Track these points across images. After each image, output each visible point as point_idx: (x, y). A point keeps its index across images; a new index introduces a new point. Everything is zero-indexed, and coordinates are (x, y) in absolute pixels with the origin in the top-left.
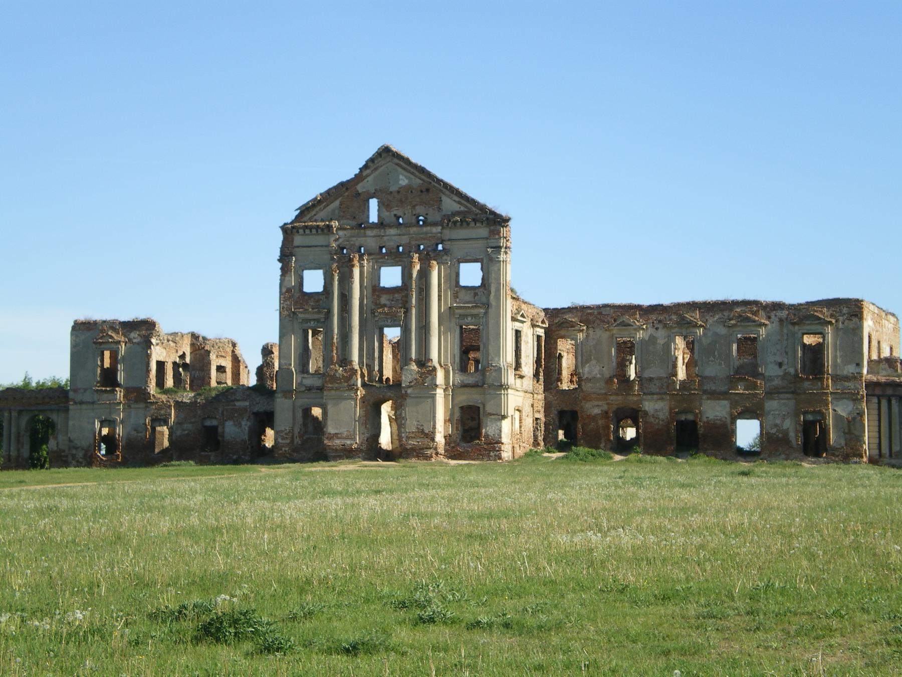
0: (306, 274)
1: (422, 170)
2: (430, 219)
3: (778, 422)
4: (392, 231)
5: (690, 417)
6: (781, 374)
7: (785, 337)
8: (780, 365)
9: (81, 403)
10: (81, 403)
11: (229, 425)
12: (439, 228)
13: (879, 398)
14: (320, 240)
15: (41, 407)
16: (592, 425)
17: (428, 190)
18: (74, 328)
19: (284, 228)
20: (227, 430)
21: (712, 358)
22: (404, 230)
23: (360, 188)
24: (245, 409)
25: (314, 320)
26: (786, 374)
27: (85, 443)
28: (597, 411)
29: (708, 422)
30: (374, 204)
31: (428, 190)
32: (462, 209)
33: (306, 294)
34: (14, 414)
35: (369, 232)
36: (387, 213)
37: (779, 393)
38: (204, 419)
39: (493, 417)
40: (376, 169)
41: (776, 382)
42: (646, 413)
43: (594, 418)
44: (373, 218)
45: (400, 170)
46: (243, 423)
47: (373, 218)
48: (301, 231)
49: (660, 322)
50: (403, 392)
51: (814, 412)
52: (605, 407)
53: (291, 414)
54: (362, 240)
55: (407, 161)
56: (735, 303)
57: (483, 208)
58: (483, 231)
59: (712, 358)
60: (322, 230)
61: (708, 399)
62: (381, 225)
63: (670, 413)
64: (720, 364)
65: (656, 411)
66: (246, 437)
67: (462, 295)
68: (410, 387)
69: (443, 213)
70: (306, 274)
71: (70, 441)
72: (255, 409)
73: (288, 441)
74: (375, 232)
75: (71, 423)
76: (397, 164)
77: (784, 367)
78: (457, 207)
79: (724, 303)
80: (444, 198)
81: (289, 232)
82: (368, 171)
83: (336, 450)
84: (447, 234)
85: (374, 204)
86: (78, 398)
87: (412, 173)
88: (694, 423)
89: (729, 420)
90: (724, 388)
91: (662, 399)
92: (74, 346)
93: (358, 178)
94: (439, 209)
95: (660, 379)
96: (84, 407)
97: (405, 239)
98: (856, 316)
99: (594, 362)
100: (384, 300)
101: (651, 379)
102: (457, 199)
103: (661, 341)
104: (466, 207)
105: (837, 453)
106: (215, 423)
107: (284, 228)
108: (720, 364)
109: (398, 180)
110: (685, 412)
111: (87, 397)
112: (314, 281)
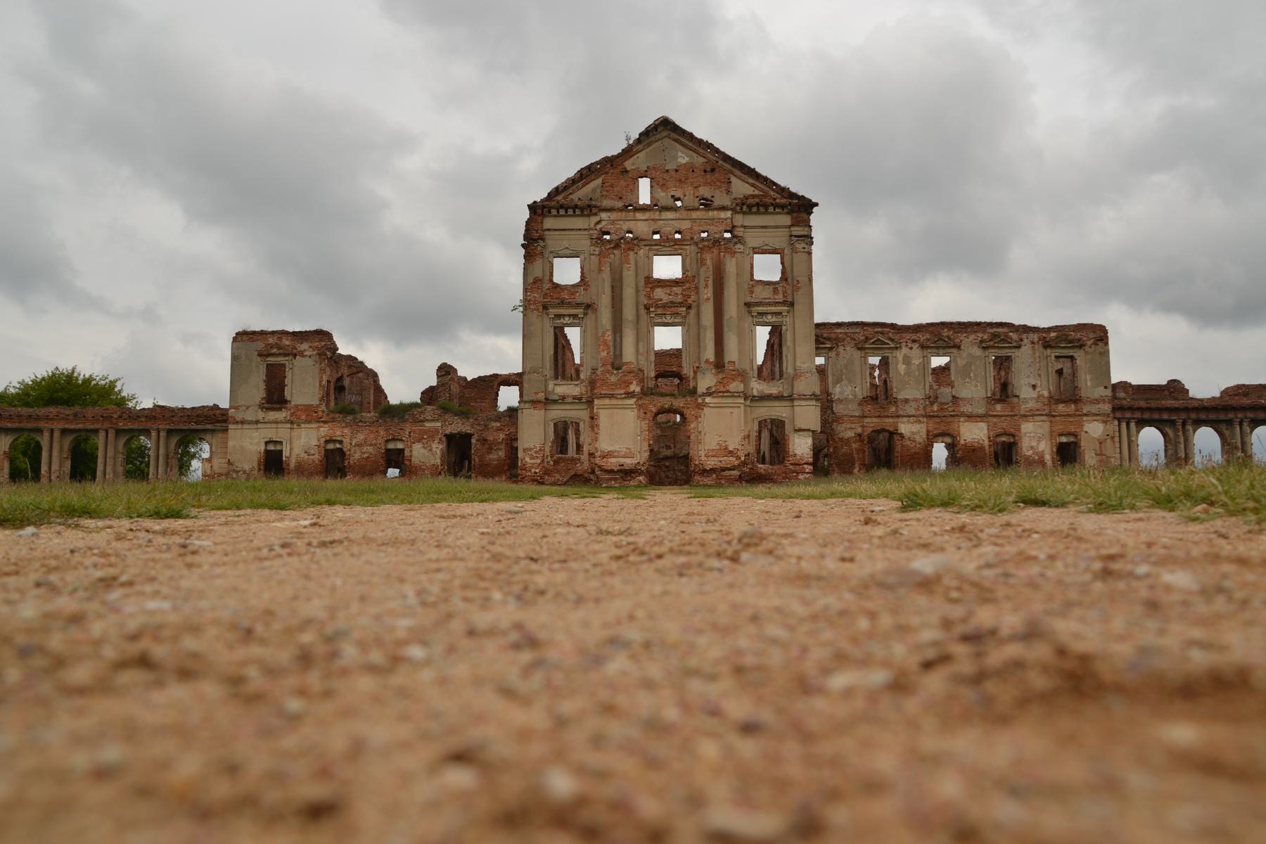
0: (557, 262)
1: (709, 146)
2: (717, 202)
3: (1034, 444)
4: (669, 215)
8: (1034, 387)
9: (243, 422)
10: (243, 422)
11: (466, 437)
12: (729, 214)
13: (1119, 420)
14: (580, 222)
15: (193, 426)
16: (845, 449)
17: (713, 170)
18: (235, 340)
19: (533, 208)
20: (415, 453)
22: (684, 214)
23: (629, 165)
24: (437, 431)
25: (569, 316)
27: (247, 467)
28: (850, 434)
30: (644, 185)
31: (713, 170)
32: (757, 192)
33: (557, 286)
34: (163, 434)
35: (639, 215)
36: (663, 194)
38: (387, 441)
40: (649, 145)
41: (1031, 405)
42: (902, 435)
43: (847, 442)
44: (644, 197)
45: (678, 146)
46: (434, 446)
47: (644, 197)
48: (554, 212)
49: (914, 341)
50: (700, 400)
51: (1069, 434)
52: (859, 430)
53: (542, 428)
54: (630, 225)
55: (691, 136)
56: (991, 325)
57: (784, 191)
58: (785, 220)
60: (582, 209)
62: (654, 206)
65: (913, 433)
66: (439, 461)
67: (758, 289)
68: (709, 394)
69: (735, 195)
70: (557, 262)
71: (229, 463)
72: (448, 432)
73: (539, 461)
74: (647, 215)
75: (230, 444)
76: (676, 140)
78: (749, 190)
79: (979, 324)
80: (733, 179)
81: (539, 211)
82: (640, 147)
83: (610, 472)
84: (739, 220)
85: (644, 185)
86: (239, 417)
87: (695, 151)
89: (986, 443)
90: (981, 411)
91: (920, 422)
92: (235, 358)
93: (628, 152)
94: (728, 192)
95: (916, 400)
96: (246, 426)
97: (685, 225)
99: (845, 382)
100: (659, 293)
101: (906, 401)
102: (751, 181)
103: (916, 362)
104: (762, 190)
106: (400, 446)
107: (533, 208)
109: (676, 157)
110: (943, 434)
111: (250, 416)
112: (567, 272)
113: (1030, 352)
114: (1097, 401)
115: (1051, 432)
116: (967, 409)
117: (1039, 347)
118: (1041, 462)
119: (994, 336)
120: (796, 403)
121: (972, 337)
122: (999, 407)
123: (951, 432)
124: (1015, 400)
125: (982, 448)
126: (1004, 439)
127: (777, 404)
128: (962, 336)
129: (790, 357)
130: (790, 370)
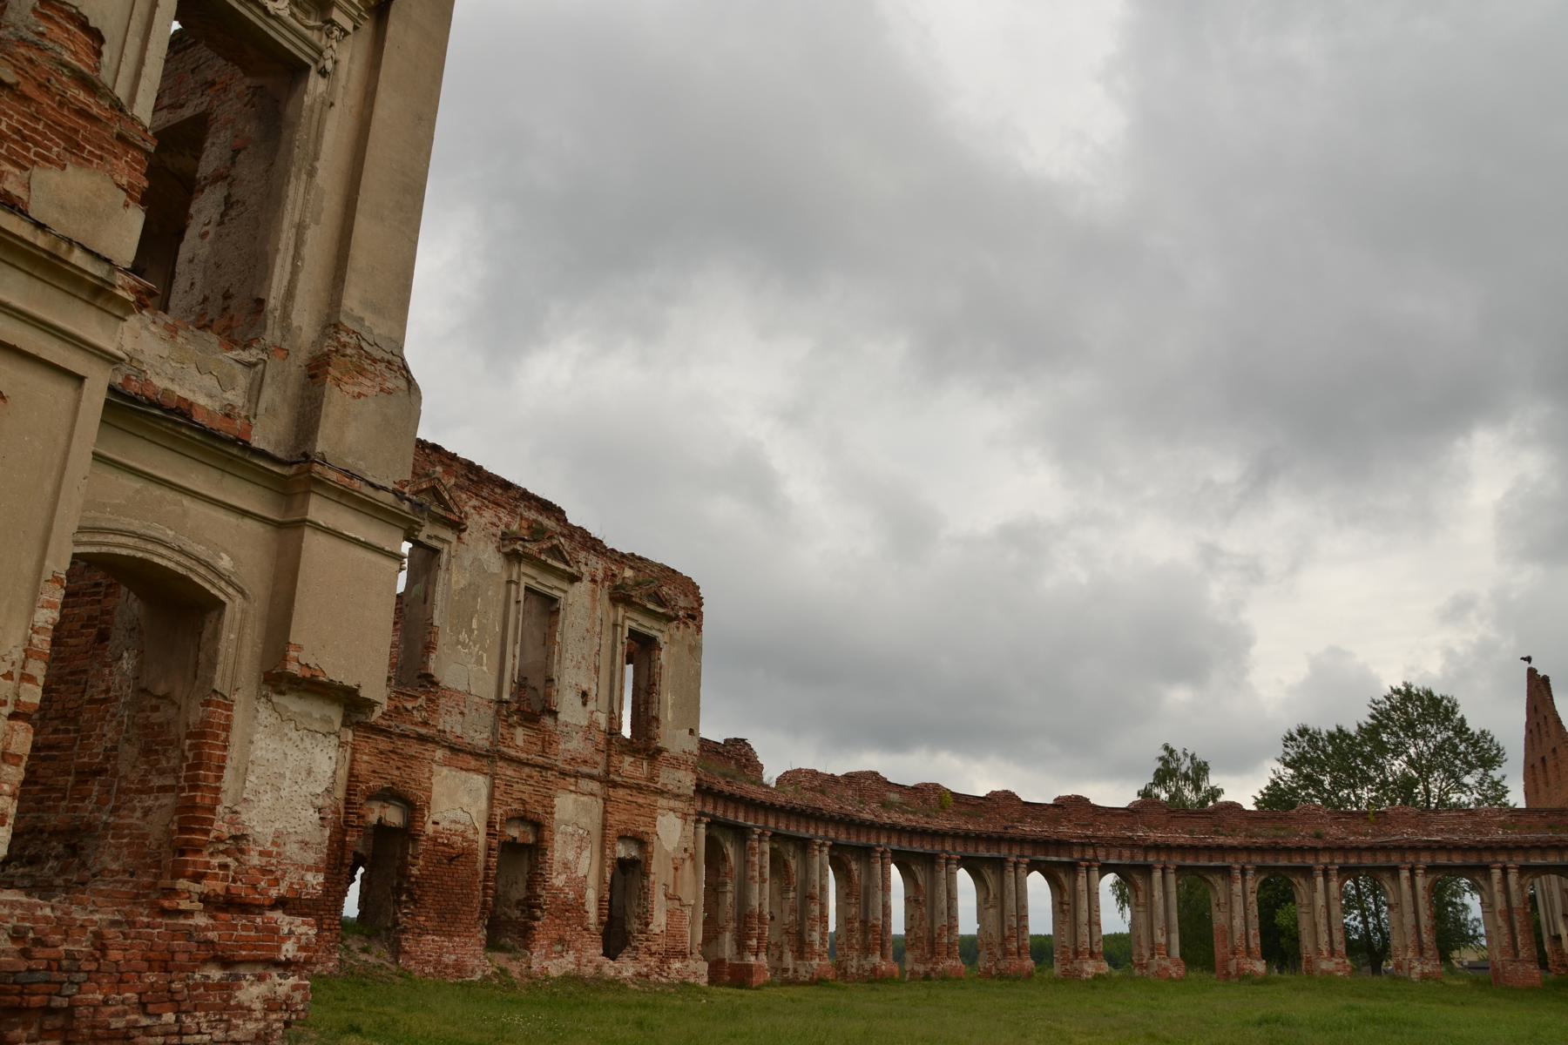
3: (571, 856)
5: (394, 816)
6: (585, 723)
7: (598, 629)
8: (584, 695)
21: (464, 636)
26: (592, 725)
29: (434, 840)
37: (577, 775)
39: (293, 704)
59: (464, 636)
61: (446, 763)
63: (350, 790)
64: (479, 661)
77: (591, 706)
79: (507, 486)
88: (407, 834)
89: (482, 839)
90: (481, 739)
98: (694, 618)
105: (654, 949)
108: (479, 661)
110: (389, 795)
113: (587, 601)
114: (676, 763)
115: (605, 826)
116: (450, 723)
117: (603, 595)
118: (578, 907)
119: (537, 533)
120: (319, 510)
121: (488, 515)
122: (520, 735)
123: (412, 790)
124: (548, 721)
125: (467, 854)
126: (514, 832)
127: (198, 478)
128: (469, 504)
129: (318, 243)
130: (305, 320)
